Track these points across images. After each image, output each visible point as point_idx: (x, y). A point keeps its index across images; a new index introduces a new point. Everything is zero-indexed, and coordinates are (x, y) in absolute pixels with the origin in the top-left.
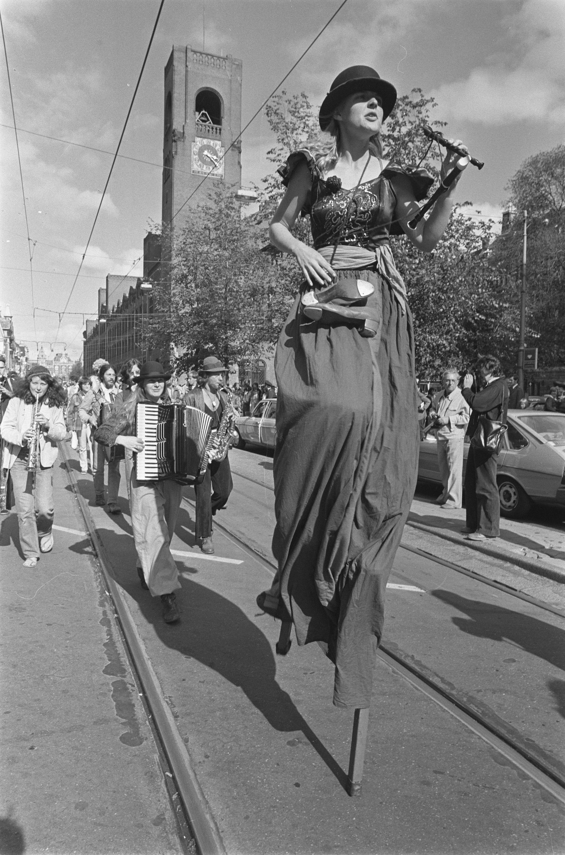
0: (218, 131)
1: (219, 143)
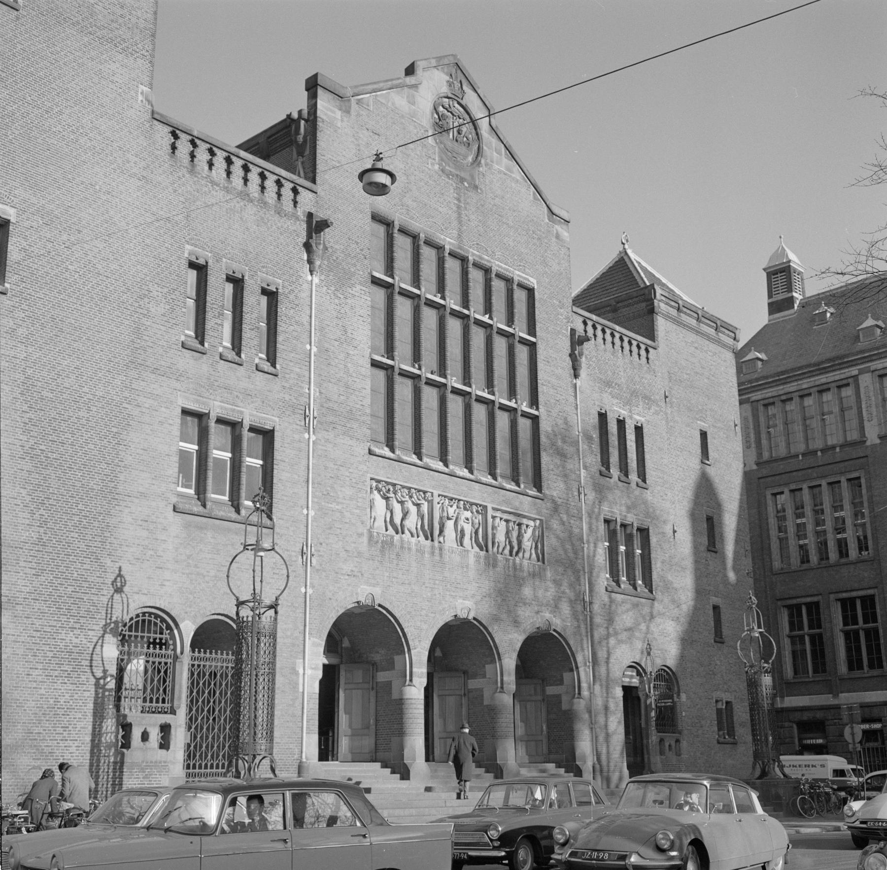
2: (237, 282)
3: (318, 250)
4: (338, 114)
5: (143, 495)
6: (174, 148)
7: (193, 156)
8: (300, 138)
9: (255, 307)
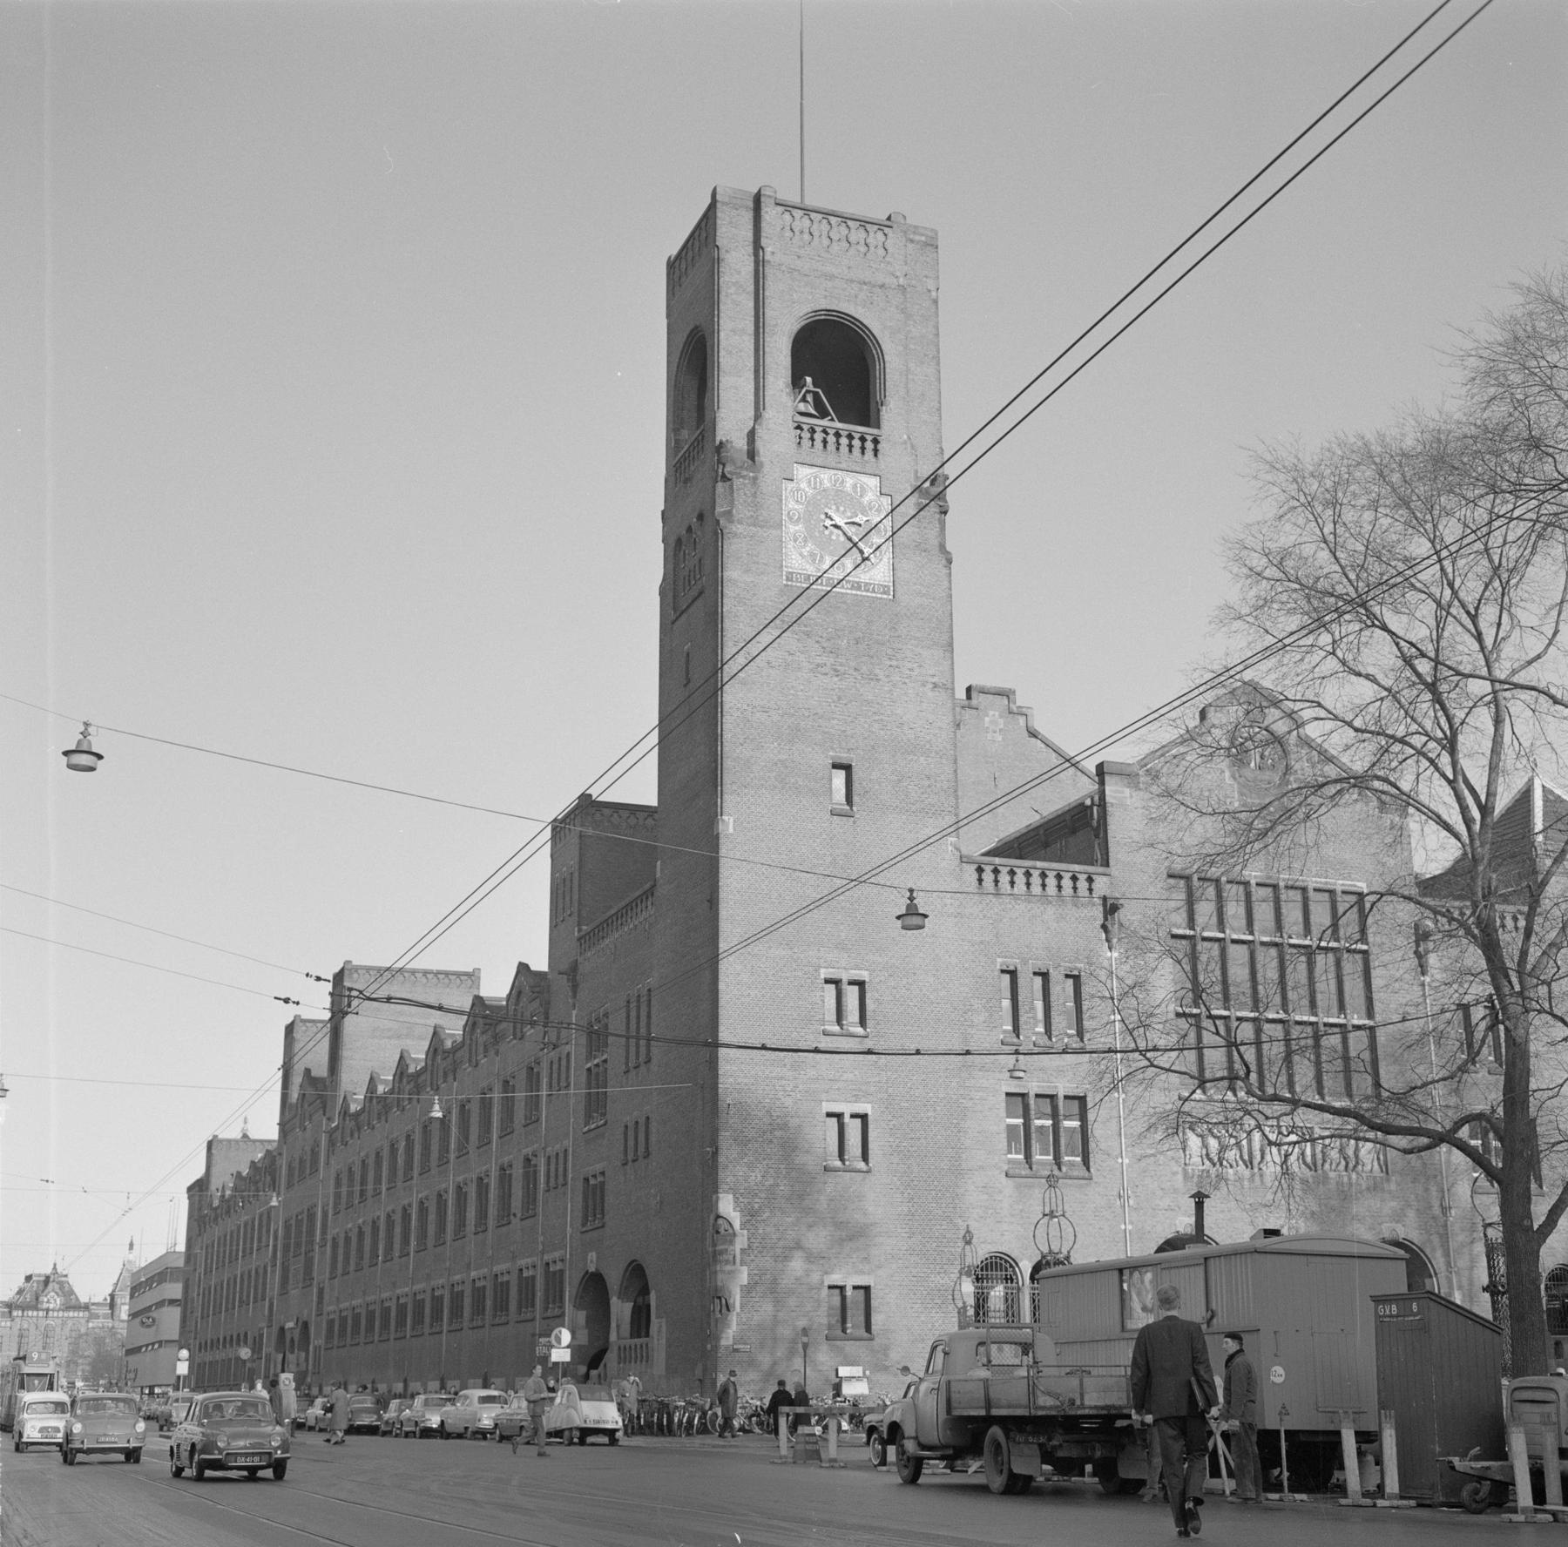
0: (869, 445)
1: (873, 482)
2: (1045, 976)
3: (1115, 929)
4: (1127, 791)
5: (982, 1167)
6: (980, 880)
7: (996, 881)
8: (1095, 823)
9: (1062, 991)
